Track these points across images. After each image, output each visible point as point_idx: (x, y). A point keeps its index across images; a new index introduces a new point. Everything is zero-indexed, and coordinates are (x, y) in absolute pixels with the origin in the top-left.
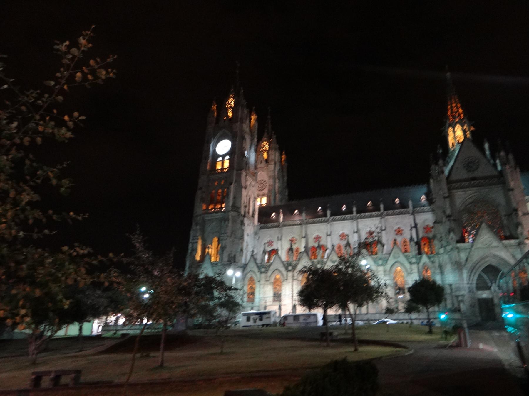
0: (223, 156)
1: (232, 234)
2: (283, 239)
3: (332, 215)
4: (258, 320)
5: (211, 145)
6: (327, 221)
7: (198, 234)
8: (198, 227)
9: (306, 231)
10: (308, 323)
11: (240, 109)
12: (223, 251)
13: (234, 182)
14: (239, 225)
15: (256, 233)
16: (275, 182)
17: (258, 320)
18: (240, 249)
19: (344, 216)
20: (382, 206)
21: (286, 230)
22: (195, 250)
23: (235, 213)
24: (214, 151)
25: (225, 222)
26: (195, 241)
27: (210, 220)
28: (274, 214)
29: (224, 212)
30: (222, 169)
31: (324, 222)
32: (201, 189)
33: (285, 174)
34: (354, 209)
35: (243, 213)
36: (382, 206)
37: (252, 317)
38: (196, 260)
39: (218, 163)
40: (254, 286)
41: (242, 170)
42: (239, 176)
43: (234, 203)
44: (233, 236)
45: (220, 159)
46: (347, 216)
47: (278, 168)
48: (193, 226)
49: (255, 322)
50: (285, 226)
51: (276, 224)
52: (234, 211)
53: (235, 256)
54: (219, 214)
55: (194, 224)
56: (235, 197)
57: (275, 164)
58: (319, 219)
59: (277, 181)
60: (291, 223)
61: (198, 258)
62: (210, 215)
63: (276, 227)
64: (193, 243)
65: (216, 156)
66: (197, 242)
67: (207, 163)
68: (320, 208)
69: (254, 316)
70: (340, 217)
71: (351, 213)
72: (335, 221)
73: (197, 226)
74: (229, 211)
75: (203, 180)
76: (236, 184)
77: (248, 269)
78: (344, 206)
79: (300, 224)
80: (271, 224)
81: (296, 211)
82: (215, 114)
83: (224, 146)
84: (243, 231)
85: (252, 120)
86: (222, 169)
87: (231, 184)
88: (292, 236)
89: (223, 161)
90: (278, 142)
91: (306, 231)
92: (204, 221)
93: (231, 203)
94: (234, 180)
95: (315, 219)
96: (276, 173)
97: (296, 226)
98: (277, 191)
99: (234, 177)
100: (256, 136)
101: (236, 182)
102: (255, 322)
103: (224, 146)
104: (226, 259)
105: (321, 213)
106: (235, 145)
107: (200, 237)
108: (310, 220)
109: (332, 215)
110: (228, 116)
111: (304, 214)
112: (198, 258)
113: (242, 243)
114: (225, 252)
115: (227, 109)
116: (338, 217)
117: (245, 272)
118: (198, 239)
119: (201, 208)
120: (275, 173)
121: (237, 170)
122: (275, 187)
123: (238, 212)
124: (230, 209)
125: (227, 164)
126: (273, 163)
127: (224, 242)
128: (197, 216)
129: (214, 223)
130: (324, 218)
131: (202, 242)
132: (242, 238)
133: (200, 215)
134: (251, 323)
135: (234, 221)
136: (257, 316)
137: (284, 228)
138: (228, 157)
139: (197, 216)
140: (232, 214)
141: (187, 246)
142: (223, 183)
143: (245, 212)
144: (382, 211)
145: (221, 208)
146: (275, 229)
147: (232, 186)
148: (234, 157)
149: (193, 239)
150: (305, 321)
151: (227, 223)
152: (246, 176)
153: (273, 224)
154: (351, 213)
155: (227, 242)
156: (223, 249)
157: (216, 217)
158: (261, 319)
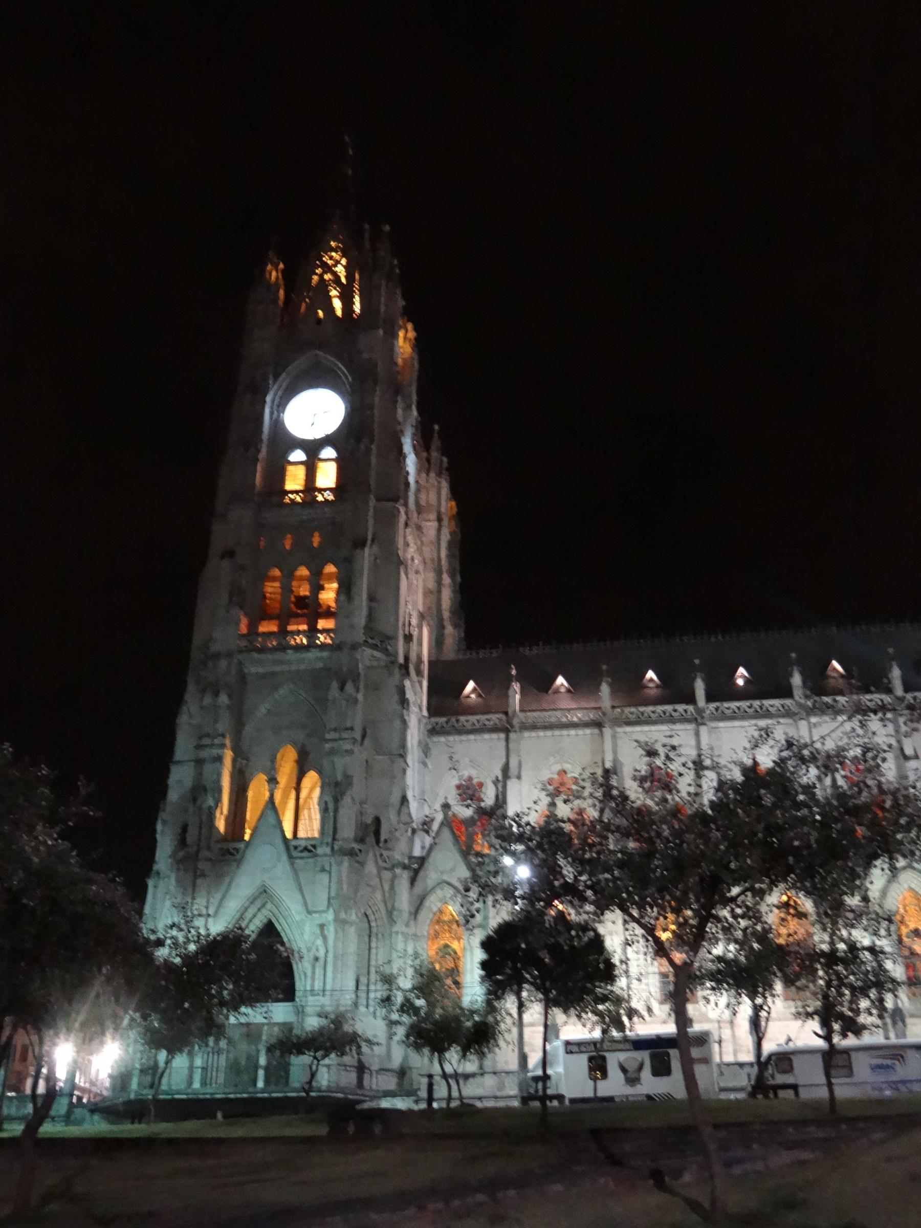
0: (313, 448)
1: (364, 736)
2: (523, 774)
3: (710, 698)
4: (646, 1073)
5: (269, 399)
6: (698, 720)
7: (220, 727)
8: (224, 699)
9: (615, 752)
10: (894, 1085)
11: (384, 282)
12: (336, 800)
13: (370, 537)
14: (393, 703)
15: (426, 750)
16: (439, 582)
17: (646, 1073)
18: (395, 799)
19: (756, 703)
20: (896, 673)
21: (530, 744)
22: (203, 790)
23: (377, 654)
24: (278, 425)
25: (342, 688)
26: (203, 754)
27: (262, 676)
28: (471, 685)
29: (336, 647)
30: (310, 486)
31: (684, 720)
32: (229, 554)
33: (457, 564)
34: (797, 680)
35: (401, 660)
36: (896, 673)
37: (613, 1060)
38: (217, 829)
39: (290, 468)
40: (455, 945)
41: (396, 500)
42: (388, 521)
43: (371, 617)
44: (367, 742)
45: (298, 455)
46: (767, 703)
47: (445, 537)
48: (188, 697)
49: (632, 1080)
50: (534, 727)
51: (494, 717)
52: (375, 647)
53: (377, 821)
54: (313, 654)
55: (191, 687)
56: (372, 599)
57: (439, 520)
58: (660, 709)
59: (446, 579)
60: (552, 717)
61: (221, 825)
62: (278, 656)
63: (494, 729)
64: (199, 762)
65: (284, 442)
66: (219, 759)
67: (256, 460)
68: (651, 674)
69: (622, 1056)
70: (744, 704)
71: (786, 692)
72: (724, 717)
73: (216, 694)
74: (354, 647)
75: (232, 525)
76: (375, 549)
77: (431, 876)
78: (742, 671)
79: (598, 725)
80: (473, 719)
81: (560, 680)
82: (282, 293)
83: (314, 412)
84: (404, 723)
85: (401, 341)
86: (310, 486)
87: (360, 544)
88: (558, 767)
89: (311, 469)
90: (444, 451)
91: (615, 752)
92: (243, 678)
93: (360, 619)
94: (370, 537)
95: (650, 708)
96: (444, 553)
97: (573, 732)
98: (446, 614)
99: (371, 523)
100: (414, 398)
101: (373, 540)
102: (632, 1080)
103: (314, 412)
104: (347, 831)
105: (653, 692)
106: (371, 407)
107: (228, 742)
108: (627, 710)
109: (710, 698)
110: (330, 309)
111: (605, 689)
112: (221, 825)
113: (404, 771)
114: (347, 800)
115: (323, 286)
116: (734, 705)
117: (418, 889)
118: (223, 746)
119: (221, 628)
120: (439, 550)
121: (378, 500)
122: (439, 600)
123: (386, 651)
124: (361, 638)
125: (327, 475)
126: (433, 516)
127: (340, 762)
128: (217, 656)
129: (282, 691)
130: (681, 707)
131: (234, 761)
132: (403, 756)
133: (230, 655)
134: (614, 1085)
135: (374, 688)
136: (644, 1056)
137: (526, 734)
138: (329, 452)
139: (217, 656)
140: (367, 657)
141: (166, 773)
142: (316, 540)
143: (407, 658)
144: (899, 692)
145: (313, 631)
146: (487, 736)
147: (367, 550)
148: (368, 451)
149: (199, 747)
150: (881, 1078)
151: (349, 687)
152: (406, 525)
153: (486, 717)
154: (786, 692)
155: (352, 763)
156: (335, 791)
157: (294, 668)
158: (661, 1069)
